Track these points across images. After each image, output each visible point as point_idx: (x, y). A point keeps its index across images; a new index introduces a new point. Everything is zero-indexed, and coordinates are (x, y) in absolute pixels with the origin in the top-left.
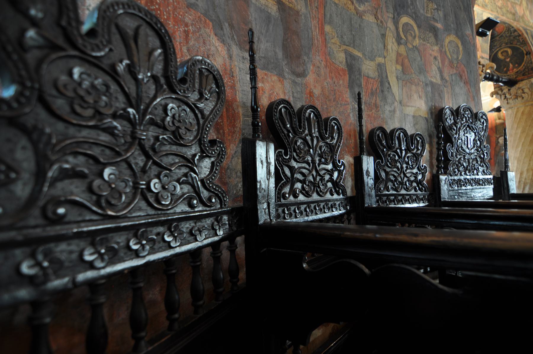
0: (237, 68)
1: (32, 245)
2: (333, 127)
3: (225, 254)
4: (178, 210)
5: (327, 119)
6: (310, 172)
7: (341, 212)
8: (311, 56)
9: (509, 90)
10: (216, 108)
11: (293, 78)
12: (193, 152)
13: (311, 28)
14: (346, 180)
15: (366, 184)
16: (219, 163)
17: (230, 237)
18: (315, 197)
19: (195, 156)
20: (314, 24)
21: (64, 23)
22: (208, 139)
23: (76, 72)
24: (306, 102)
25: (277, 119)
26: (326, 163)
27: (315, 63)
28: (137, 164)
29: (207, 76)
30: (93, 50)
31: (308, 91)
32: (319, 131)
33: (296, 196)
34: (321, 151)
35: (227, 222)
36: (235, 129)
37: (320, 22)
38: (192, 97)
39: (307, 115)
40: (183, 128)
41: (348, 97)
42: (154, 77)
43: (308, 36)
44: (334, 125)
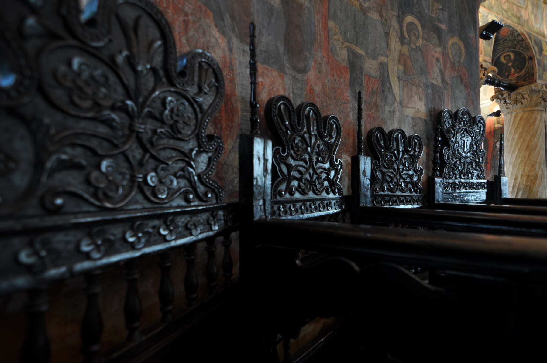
0: (237, 62)
1: (31, 234)
2: (332, 126)
3: (220, 250)
4: (174, 204)
5: (326, 118)
6: (307, 170)
7: (336, 211)
8: (313, 52)
9: (509, 95)
10: (215, 103)
12: (190, 146)
14: (343, 180)
15: (362, 184)
18: (311, 195)
19: (192, 150)
21: (64, 11)
22: (206, 133)
23: (76, 62)
26: (324, 162)
28: (134, 157)
29: (207, 70)
30: (93, 40)
33: (292, 194)
34: (319, 149)
35: (222, 218)
36: (233, 124)
38: (191, 90)
39: (306, 112)
40: (181, 122)
41: (348, 95)
42: (153, 70)
44: (333, 123)
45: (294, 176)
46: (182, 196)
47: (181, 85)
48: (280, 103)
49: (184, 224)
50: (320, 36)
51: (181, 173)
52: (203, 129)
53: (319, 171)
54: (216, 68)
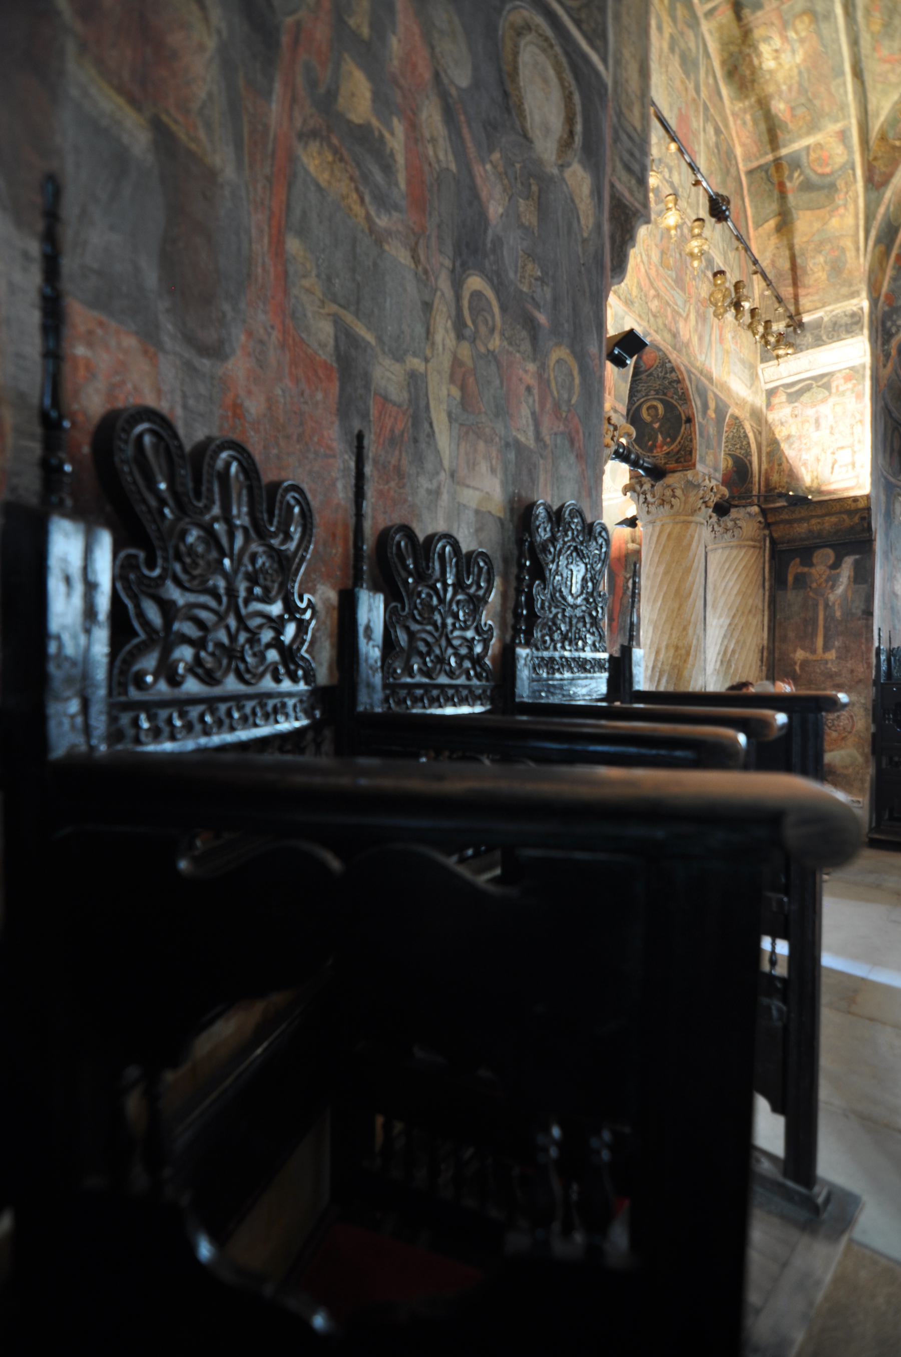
2: (290, 508)
5: (274, 487)
6: (221, 617)
7: (297, 724)
8: (242, 305)
9: (653, 486)
11: (189, 354)
14: (317, 646)
15: (362, 658)
18: (231, 684)
26: (267, 599)
32: (252, 514)
33: (175, 681)
39: (220, 464)
41: (333, 435)
44: (292, 502)
50: (264, 269)
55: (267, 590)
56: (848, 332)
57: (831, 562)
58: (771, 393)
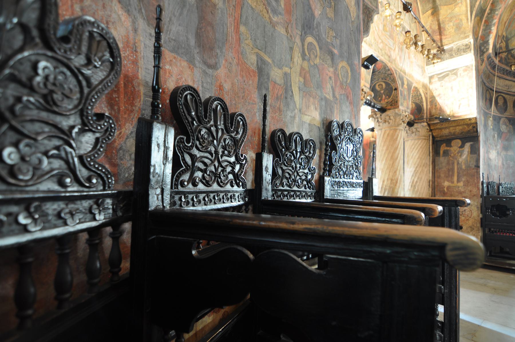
0: (143, 44)
2: (239, 122)
3: (108, 242)
5: (233, 115)
6: (213, 162)
7: (239, 203)
8: (224, 51)
10: (108, 79)
11: (205, 68)
12: (71, 121)
13: (226, 24)
14: (247, 174)
16: (106, 141)
17: (114, 223)
18: (215, 187)
19: (73, 127)
20: (229, 21)
24: (215, 94)
25: (181, 105)
26: (229, 156)
27: (226, 58)
29: (99, 42)
31: (218, 84)
32: (225, 124)
33: (195, 185)
34: (225, 142)
35: (111, 207)
36: (134, 108)
37: (236, 21)
39: (214, 106)
43: (223, 31)
44: (240, 120)
45: (199, 167)
46: (55, 179)
47: (63, 51)
48: (186, 93)
49: (55, 212)
50: (232, 38)
51: (55, 152)
52: (90, 105)
53: (224, 164)
54: (112, 43)
55: (229, 152)
56: (464, 52)
57: (460, 145)
58: (431, 78)
